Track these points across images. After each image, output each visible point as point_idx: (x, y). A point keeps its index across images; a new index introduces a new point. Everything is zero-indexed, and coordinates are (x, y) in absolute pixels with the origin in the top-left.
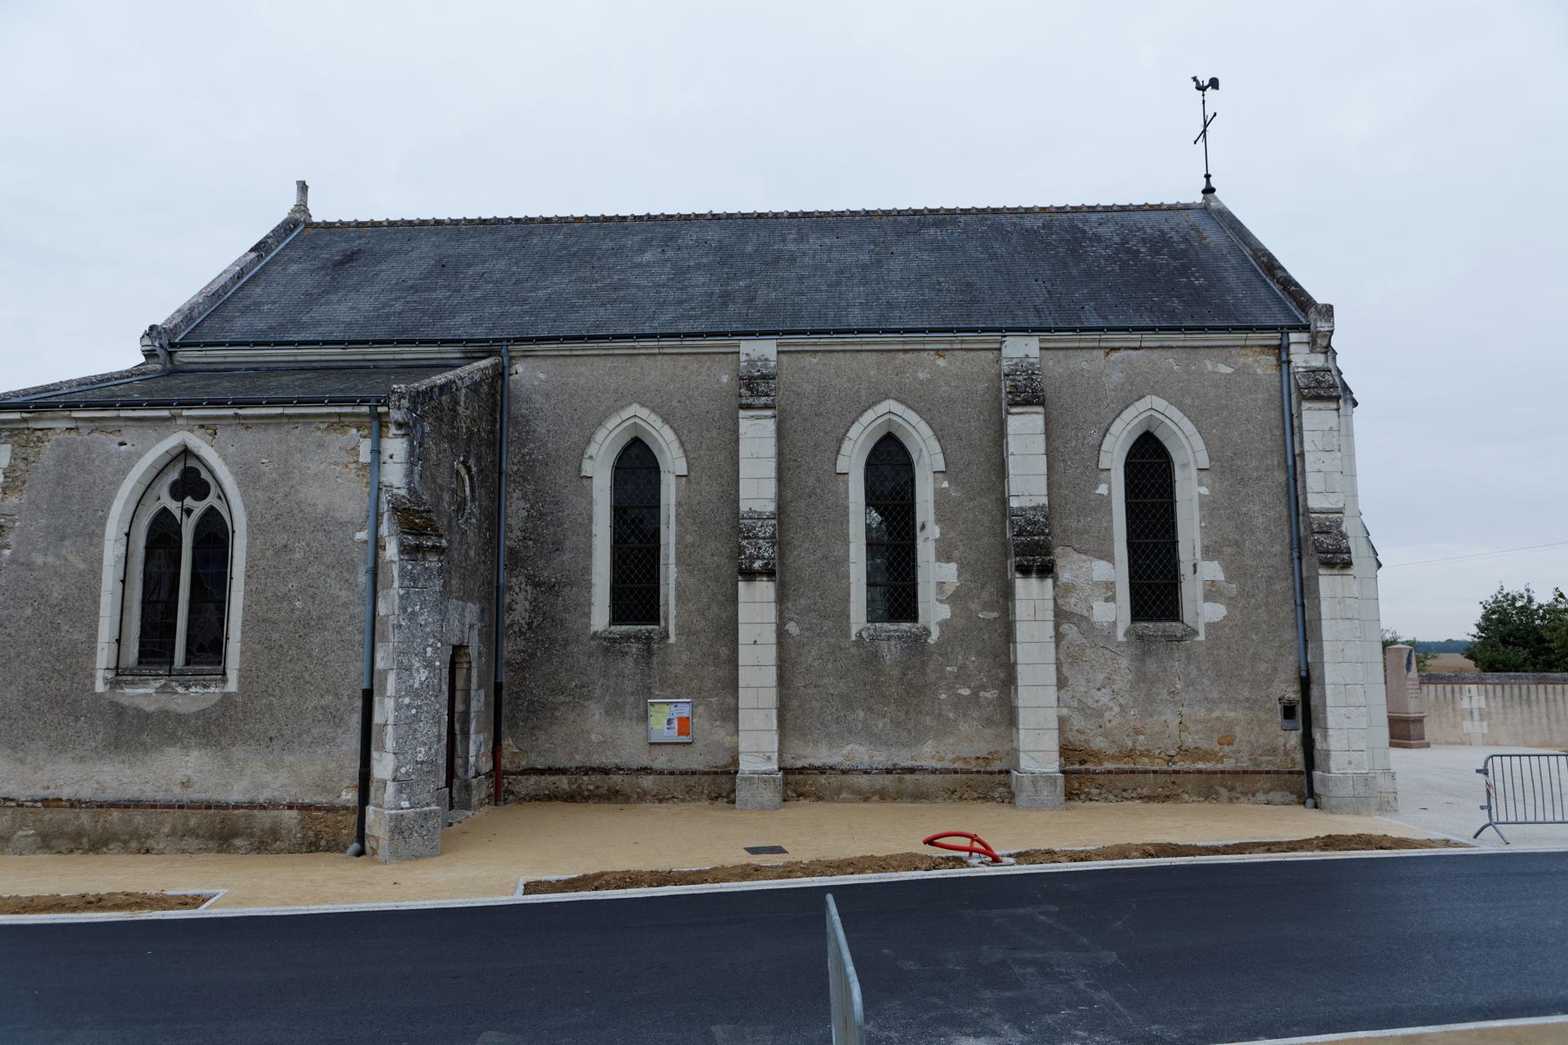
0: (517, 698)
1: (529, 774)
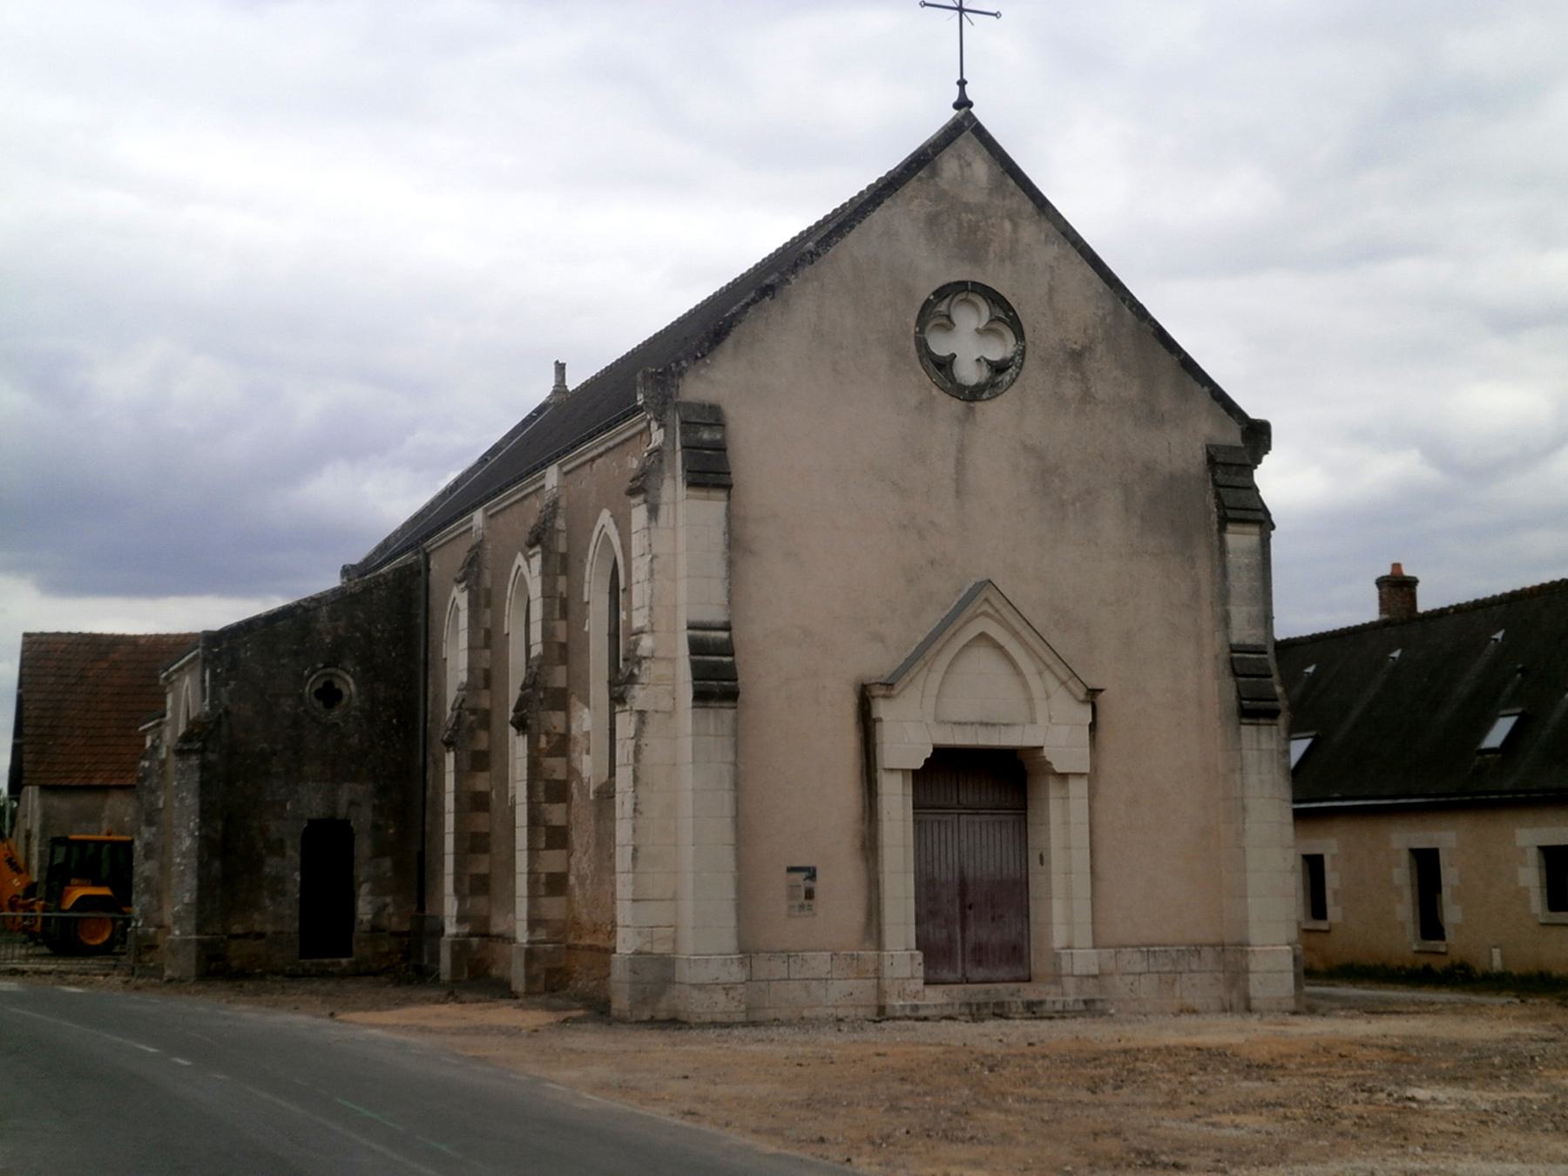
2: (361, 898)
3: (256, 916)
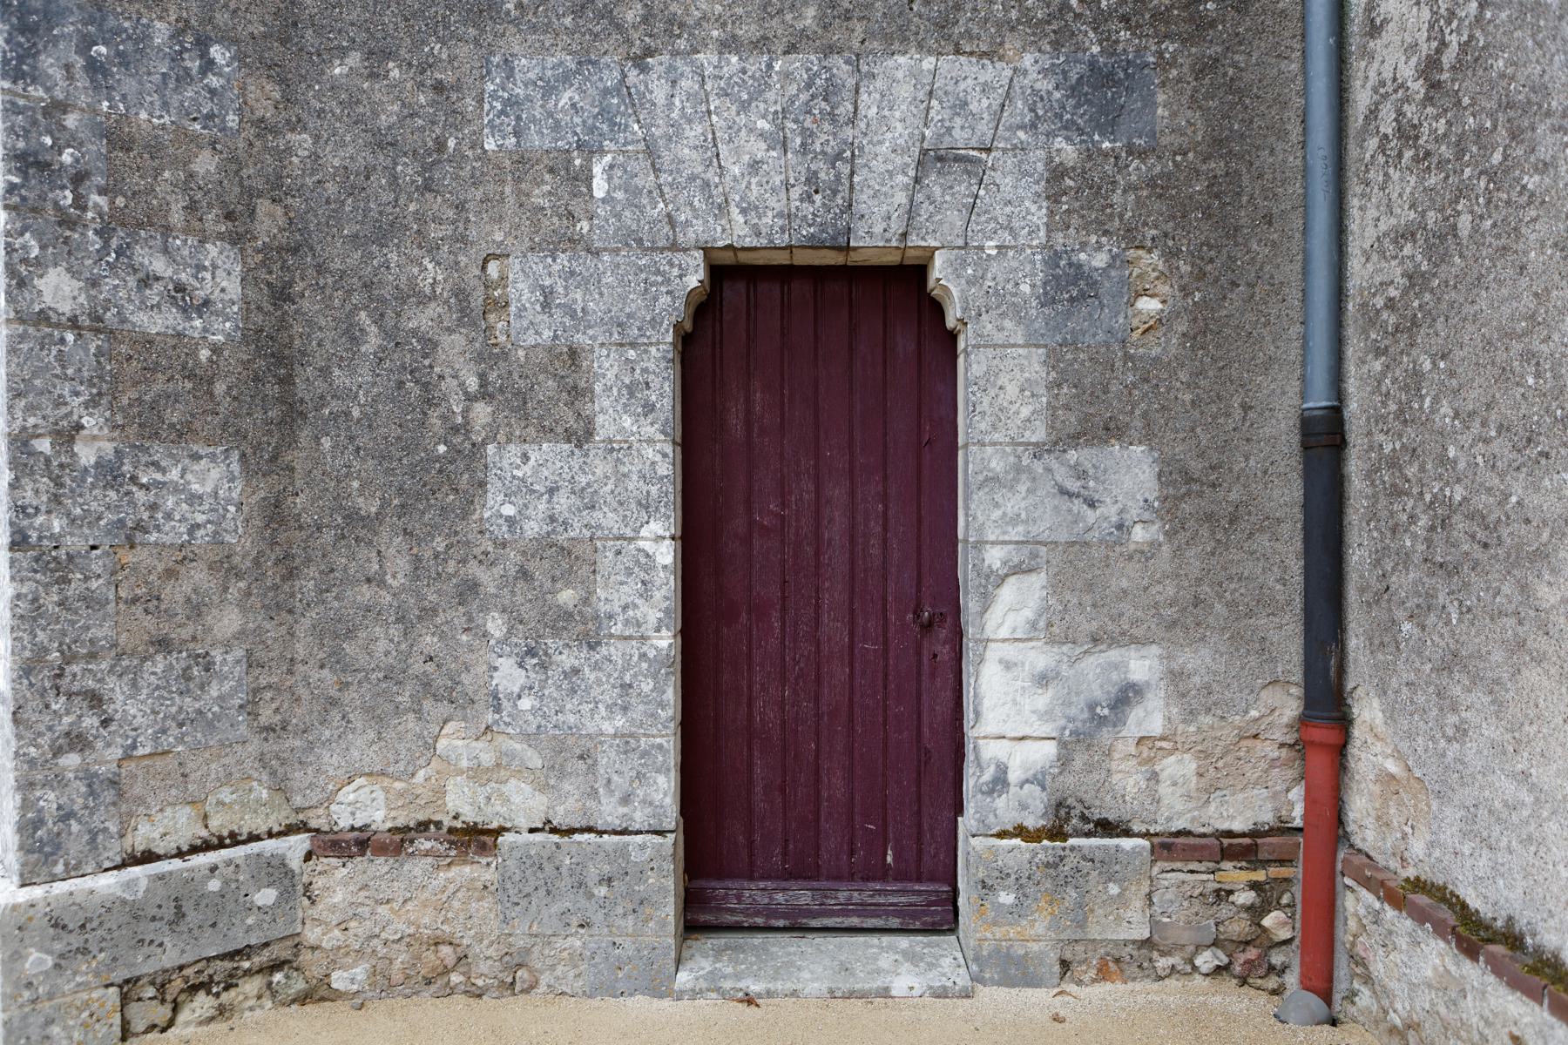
0: (1396, 492)
1: (1420, 916)
2: (994, 652)
3: (454, 742)
